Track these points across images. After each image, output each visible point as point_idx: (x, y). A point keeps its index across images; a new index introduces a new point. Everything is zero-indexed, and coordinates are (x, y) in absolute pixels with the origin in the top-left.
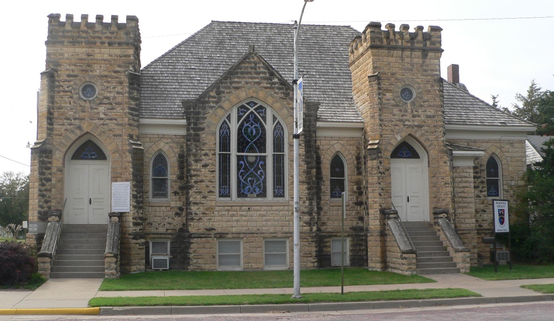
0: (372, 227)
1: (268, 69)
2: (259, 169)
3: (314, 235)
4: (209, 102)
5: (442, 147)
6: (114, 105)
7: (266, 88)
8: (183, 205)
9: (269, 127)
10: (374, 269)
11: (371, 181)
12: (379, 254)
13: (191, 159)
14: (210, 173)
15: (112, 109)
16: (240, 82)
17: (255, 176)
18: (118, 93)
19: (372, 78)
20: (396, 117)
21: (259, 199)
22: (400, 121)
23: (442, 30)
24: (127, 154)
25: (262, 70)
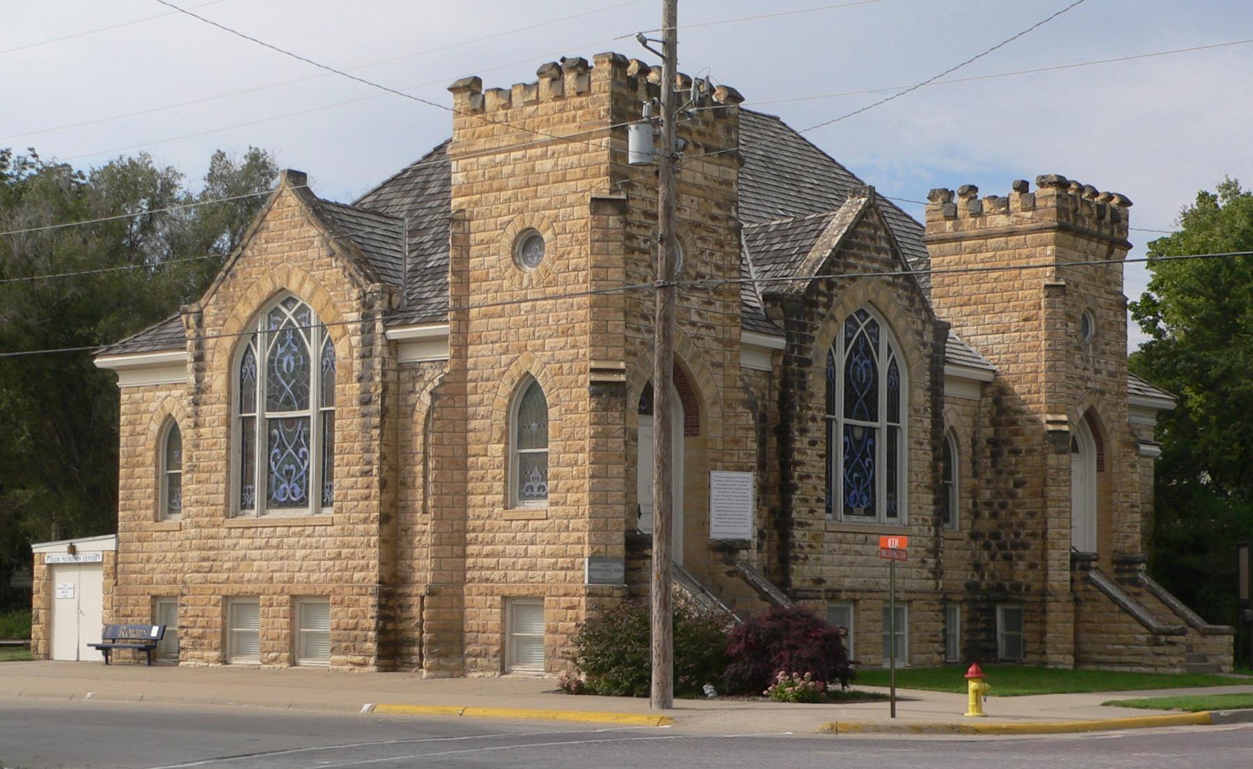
0: (1055, 584)
1: (892, 246)
2: (868, 456)
3: (941, 596)
4: (815, 304)
5: (1127, 436)
6: (711, 293)
7: (889, 284)
8: (765, 528)
9: (883, 366)
10: (1061, 667)
11: (1054, 494)
12: (1071, 636)
13: (795, 425)
14: (819, 459)
15: (709, 303)
16: (855, 267)
17: (863, 470)
18: (718, 268)
19: (1053, 290)
20: (1078, 371)
21: (868, 519)
22: (1082, 378)
23: (1131, 204)
24: (740, 409)
25: (884, 244)
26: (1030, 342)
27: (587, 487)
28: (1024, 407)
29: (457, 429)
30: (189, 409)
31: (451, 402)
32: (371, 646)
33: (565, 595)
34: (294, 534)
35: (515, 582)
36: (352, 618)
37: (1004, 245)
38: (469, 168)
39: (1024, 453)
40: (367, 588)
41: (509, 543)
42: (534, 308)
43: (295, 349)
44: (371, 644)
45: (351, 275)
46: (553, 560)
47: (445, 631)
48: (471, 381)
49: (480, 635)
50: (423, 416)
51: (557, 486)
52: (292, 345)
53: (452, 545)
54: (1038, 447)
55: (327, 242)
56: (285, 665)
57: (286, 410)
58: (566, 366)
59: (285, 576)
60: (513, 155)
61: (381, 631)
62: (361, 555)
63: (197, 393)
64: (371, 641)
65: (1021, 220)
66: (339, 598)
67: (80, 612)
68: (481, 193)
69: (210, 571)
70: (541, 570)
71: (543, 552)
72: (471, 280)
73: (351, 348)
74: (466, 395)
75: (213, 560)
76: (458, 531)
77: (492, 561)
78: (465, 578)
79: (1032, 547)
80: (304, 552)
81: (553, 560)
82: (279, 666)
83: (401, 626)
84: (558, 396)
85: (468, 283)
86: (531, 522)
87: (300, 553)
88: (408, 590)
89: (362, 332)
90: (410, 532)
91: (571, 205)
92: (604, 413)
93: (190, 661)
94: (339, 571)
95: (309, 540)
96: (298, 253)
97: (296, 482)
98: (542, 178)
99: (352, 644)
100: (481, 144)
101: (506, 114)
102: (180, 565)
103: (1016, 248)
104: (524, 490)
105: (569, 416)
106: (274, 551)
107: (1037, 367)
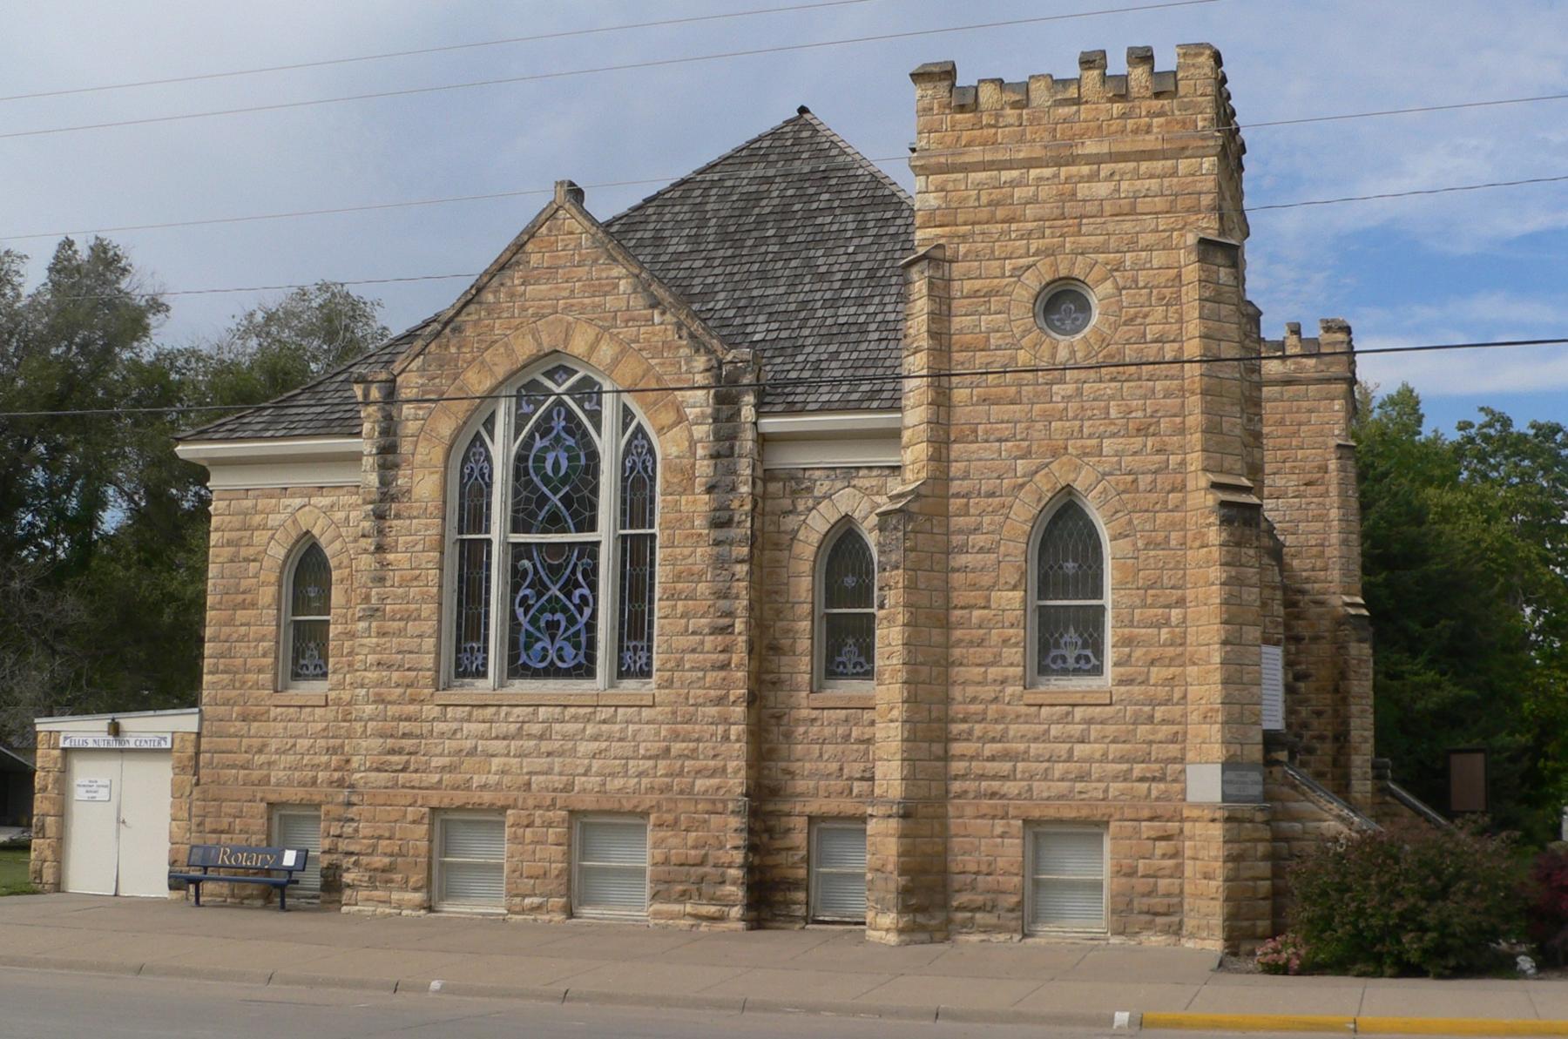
0: (1358, 796)
19: (1345, 451)
26: (1314, 510)
27: (1217, 659)
28: (1308, 586)
29: (936, 567)
30: (367, 525)
31: (928, 525)
32: (736, 892)
33: (1151, 819)
34: (575, 719)
35: (1048, 798)
36: (695, 847)
37: (1278, 396)
38: (950, 186)
39: (1307, 641)
40: (724, 802)
41: (1036, 740)
42: (1079, 392)
43: (570, 442)
44: (734, 888)
45: (692, 336)
46: (1125, 766)
47: (925, 872)
48: (957, 495)
49: (980, 878)
50: (814, 549)
51: (1130, 656)
52: (563, 434)
53: (931, 741)
54: (1326, 634)
55: (646, 287)
56: (559, 917)
57: (549, 532)
58: (1147, 479)
59: (558, 781)
60: (1034, 173)
61: (749, 868)
62: (712, 753)
63: (381, 501)
64: (734, 883)
65: (1301, 369)
66: (669, 817)
67: (121, 822)
68: (973, 224)
69: (403, 770)
70: (1099, 780)
71: (1105, 754)
72: (955, 348)
73: (693, 444)
74: (947, 517)
75: (410, 754)
76: (939, 720)
77: (1006, 767)
78: (947, 792)
79: (1319, 752)
80: (595, 746)
81: (1125, 766)
82: (547, 917)
83: (780, 859)
84: (1130, 522)
85: (950, 352)
86: (1077, 709)
87: (584, 747)
88: (786, 807)
89: (716, 420)
90: (785, 719)
91: (1149, 249)
92: (1237, 549)
93: (360, 904)
94: (666, 775)
95: (604, 727)
96: (587, 301)
97: (568, 639)
98: (1091, 208)
99: (694, 887)
100: (976, 155)
101: (1020, 116)
102: (325, 758)
103: (1291, 400)
104: (1049, 661)
105: (1152, 553)
106: (532, 743)
107: (1324, 539)
